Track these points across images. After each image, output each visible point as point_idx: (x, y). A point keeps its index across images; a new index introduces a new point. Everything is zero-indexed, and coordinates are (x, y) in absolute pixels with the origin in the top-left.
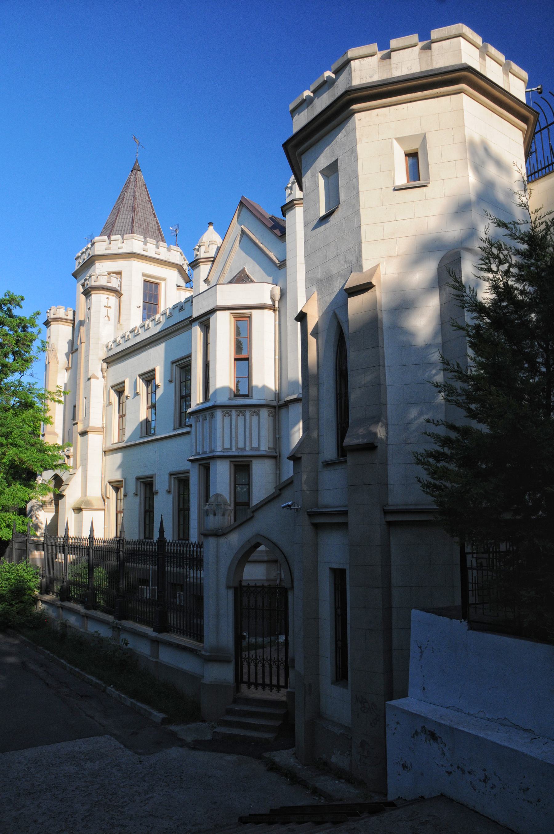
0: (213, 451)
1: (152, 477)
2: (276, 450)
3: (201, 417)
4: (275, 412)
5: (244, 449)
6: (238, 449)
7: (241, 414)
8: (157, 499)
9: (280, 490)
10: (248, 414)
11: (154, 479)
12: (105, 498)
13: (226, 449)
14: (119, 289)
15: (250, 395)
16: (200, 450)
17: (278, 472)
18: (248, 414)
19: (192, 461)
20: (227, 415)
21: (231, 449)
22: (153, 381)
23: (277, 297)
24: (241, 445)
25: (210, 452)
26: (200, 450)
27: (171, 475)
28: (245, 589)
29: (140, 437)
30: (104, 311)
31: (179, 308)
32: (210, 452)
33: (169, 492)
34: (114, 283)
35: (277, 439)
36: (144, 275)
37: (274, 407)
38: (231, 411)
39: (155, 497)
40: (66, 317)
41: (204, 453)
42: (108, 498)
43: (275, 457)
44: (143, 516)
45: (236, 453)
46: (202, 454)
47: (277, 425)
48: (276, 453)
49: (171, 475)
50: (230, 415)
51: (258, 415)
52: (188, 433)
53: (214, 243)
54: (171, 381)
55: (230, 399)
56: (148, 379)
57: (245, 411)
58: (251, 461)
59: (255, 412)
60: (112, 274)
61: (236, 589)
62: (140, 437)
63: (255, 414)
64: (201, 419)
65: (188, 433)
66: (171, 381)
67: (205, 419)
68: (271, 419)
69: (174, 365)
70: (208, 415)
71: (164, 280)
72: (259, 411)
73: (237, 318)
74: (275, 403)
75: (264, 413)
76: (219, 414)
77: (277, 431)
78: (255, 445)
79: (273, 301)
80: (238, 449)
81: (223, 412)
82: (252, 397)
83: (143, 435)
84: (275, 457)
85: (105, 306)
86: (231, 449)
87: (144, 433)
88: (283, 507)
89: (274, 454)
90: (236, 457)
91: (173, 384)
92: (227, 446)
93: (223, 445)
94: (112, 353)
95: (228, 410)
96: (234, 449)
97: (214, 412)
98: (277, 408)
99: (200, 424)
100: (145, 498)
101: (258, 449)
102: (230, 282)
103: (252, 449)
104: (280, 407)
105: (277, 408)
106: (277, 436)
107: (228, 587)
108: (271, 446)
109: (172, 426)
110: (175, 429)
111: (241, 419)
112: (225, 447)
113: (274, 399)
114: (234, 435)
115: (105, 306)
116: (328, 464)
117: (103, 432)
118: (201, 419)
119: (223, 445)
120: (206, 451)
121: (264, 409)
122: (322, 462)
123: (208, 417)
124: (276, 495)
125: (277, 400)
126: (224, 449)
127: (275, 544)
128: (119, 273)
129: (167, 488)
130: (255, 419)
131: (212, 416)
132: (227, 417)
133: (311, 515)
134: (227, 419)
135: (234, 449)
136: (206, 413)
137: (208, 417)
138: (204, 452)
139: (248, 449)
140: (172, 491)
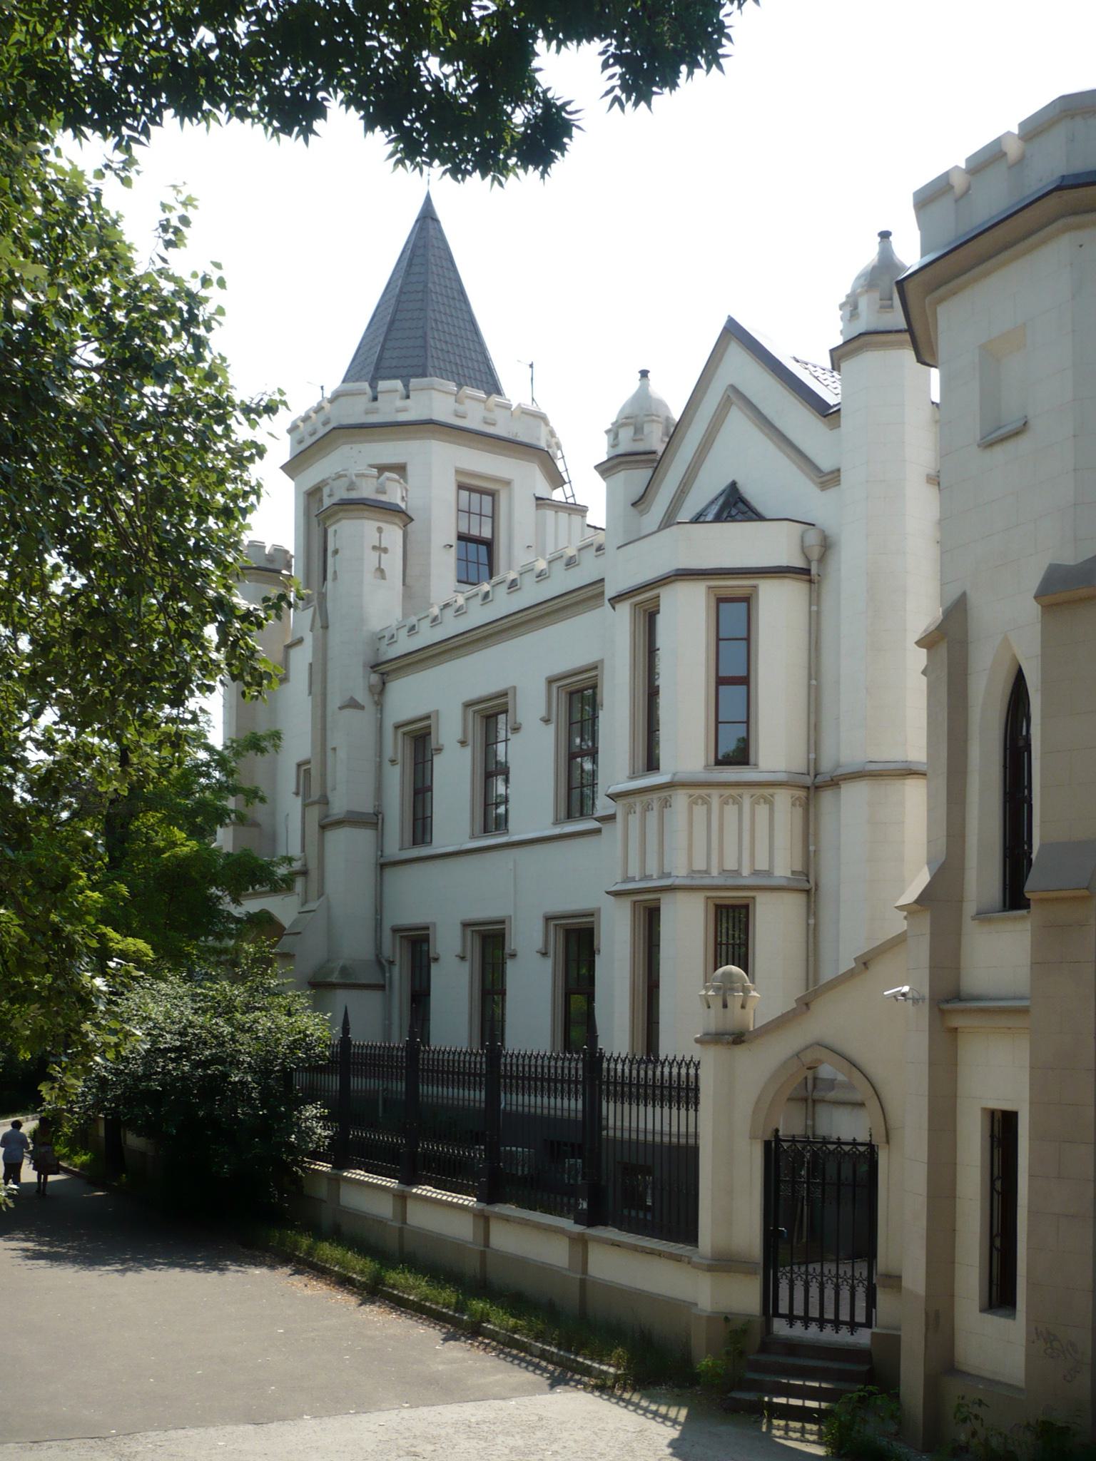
1: (503, 922)
5: (737, 873)
6: (723, 871)
11: (506, 926)
12: (382, 964)
22: (502, 718)
27: (548, 919)
30: (371, 558)
38: (709, 796)
39: (510, 965)
44: (477, 1002)
46: (640, 880)
49: (548, 919)
58: (754, 898)
76: (680, 799)
78: (762, 865)
80: (723, 871)
81: (690, 796)
85: (374, 548)
91: (552, 727)
97: (670, 796)
101: (769, 873)
103: (756, 873)
111: (731, 810)
115: (374, 548)
117: (377, 823)
120: (652, 876)
134: (700, 810)
138: (646, 876)
139: (746, 872)
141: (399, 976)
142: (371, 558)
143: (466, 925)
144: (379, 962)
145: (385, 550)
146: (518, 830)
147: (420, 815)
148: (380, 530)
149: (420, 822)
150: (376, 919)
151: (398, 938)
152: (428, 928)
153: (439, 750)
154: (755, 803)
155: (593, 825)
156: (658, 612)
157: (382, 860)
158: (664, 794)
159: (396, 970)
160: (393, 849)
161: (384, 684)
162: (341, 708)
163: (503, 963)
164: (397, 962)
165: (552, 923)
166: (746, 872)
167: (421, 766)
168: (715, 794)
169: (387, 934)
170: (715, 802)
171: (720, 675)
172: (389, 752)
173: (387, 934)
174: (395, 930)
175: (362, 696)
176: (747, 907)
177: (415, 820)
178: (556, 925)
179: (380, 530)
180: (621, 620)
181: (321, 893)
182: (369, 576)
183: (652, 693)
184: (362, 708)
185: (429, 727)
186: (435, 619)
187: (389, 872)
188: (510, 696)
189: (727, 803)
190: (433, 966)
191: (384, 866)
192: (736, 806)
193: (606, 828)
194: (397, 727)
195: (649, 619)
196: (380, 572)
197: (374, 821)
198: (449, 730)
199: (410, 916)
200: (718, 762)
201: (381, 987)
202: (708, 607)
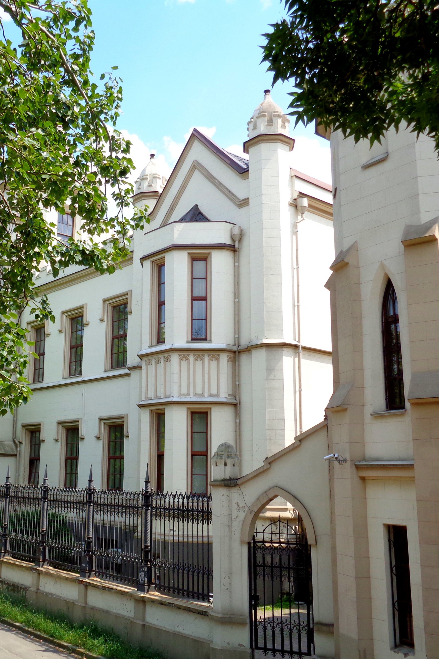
2: (235, 397)
3: (153, 360)
4: (235, 357)
5: (202, 395)
7: (199, 359)
8: (82, 446)
9: (300, 441)
10: (206, 359)
11: (80, 424)
12: (17, 443)
13: (184, 394)
15: (209, 338)
16: (151, 394)
17: (238, 421)
18: (206, 359)
19: (141, 406)
20: (184, 359)
21: (188, 395)
23: (237, 238)
24: (199, 391)
27: (101, 420)
28: (259, 545)
29: (63, 379)
32: (165, 398)
35: (237, 385)
37: (235, 352)
38: (188, 355)
39: (81, 444)
42: (20, 443)
43: (235, 405)
45: (194, 399)
47: (237, 370)
48: (236, 400)
49: (101, 420)
50: (187, 359)
51: (217, 360)
52: (128, 375)
53: (158, 176)
55: (188, 342)
56: (73, 317)
57: (203, 356)
58: (210, 408)
59: (213, 357)
61: (249, 544)
62: (63, 379)
63: (214, 359)
64: (153, 362)
65: (128, 375)
66: (102, 320)
67: (158, 362)
68: (230, 363)
69: (106, 304)
70: (162, 358)
72: (219, 355)
73: (194, 259)
74: (235, 348)
75: (224, 358)
76: (175, 358)
77: (237, 377)
78: (214, 391)
79: (234, 241)
81: (180, 356)
82: (211, 341)
83: (66, 376)
84: (235, 405)
86: (188, 395)
89: (234, 401)
90: (190, 403)
92: (184, 391)
93: (180, 390)
95: (186, 353)
96: (192, 395)
98: (237, 353)
99: (151, 368)
100: (67, 444)
101: (217, 395)
102: (182, 220)
103: (211, 395)
104: (239, 352)
105: (237, 353)
106: (237, 383)
107: (242, 542)
108: (230, 393)
109: (103, 368)
110: (106, 371)
111: (199, 363)
113: (233, 344)
114: (191, 380)
116: (377, 416)
118: (153, 362)
119: (180, 390)
121: (224, 354)
122: (371, 415)
123: (162, 361)
124: (295, 445)
125: (237, 345)
127: (295, 497)
129: (96, 432)
130: (214, 363)
131: (168, 359)
132: (184, 361)
133: (358, 467)
134: (184, 363)
135: (192, 395)
136: (160, 356)
137: (162, 361)
139: (206, 394)
140: (102, 437)
143: (59, 423)
146: (87, 374)
147: (37, 367)
149: (37, 371)
150: (14, 420)
151: (24, 430)
153: (49, 335)
155: (126, 371)
156: (164, 265)
158: (166, 355)
159: (23, 446)
163: (78, 444)
164: (23, 442)
166: (206, 394)
167: (39, 343)
169: (19, 427)
171: (193, 296)
174: (23, 426)
176: (206, 413)
177: (35, 370)
178: (105, 423)
183: (161, 304)
190: (42, 444)
192: (202, 361)
193: (135, 374)
199: (31, 420)
200: (193, 339)
201: (16, 455)
202: (188, 263)
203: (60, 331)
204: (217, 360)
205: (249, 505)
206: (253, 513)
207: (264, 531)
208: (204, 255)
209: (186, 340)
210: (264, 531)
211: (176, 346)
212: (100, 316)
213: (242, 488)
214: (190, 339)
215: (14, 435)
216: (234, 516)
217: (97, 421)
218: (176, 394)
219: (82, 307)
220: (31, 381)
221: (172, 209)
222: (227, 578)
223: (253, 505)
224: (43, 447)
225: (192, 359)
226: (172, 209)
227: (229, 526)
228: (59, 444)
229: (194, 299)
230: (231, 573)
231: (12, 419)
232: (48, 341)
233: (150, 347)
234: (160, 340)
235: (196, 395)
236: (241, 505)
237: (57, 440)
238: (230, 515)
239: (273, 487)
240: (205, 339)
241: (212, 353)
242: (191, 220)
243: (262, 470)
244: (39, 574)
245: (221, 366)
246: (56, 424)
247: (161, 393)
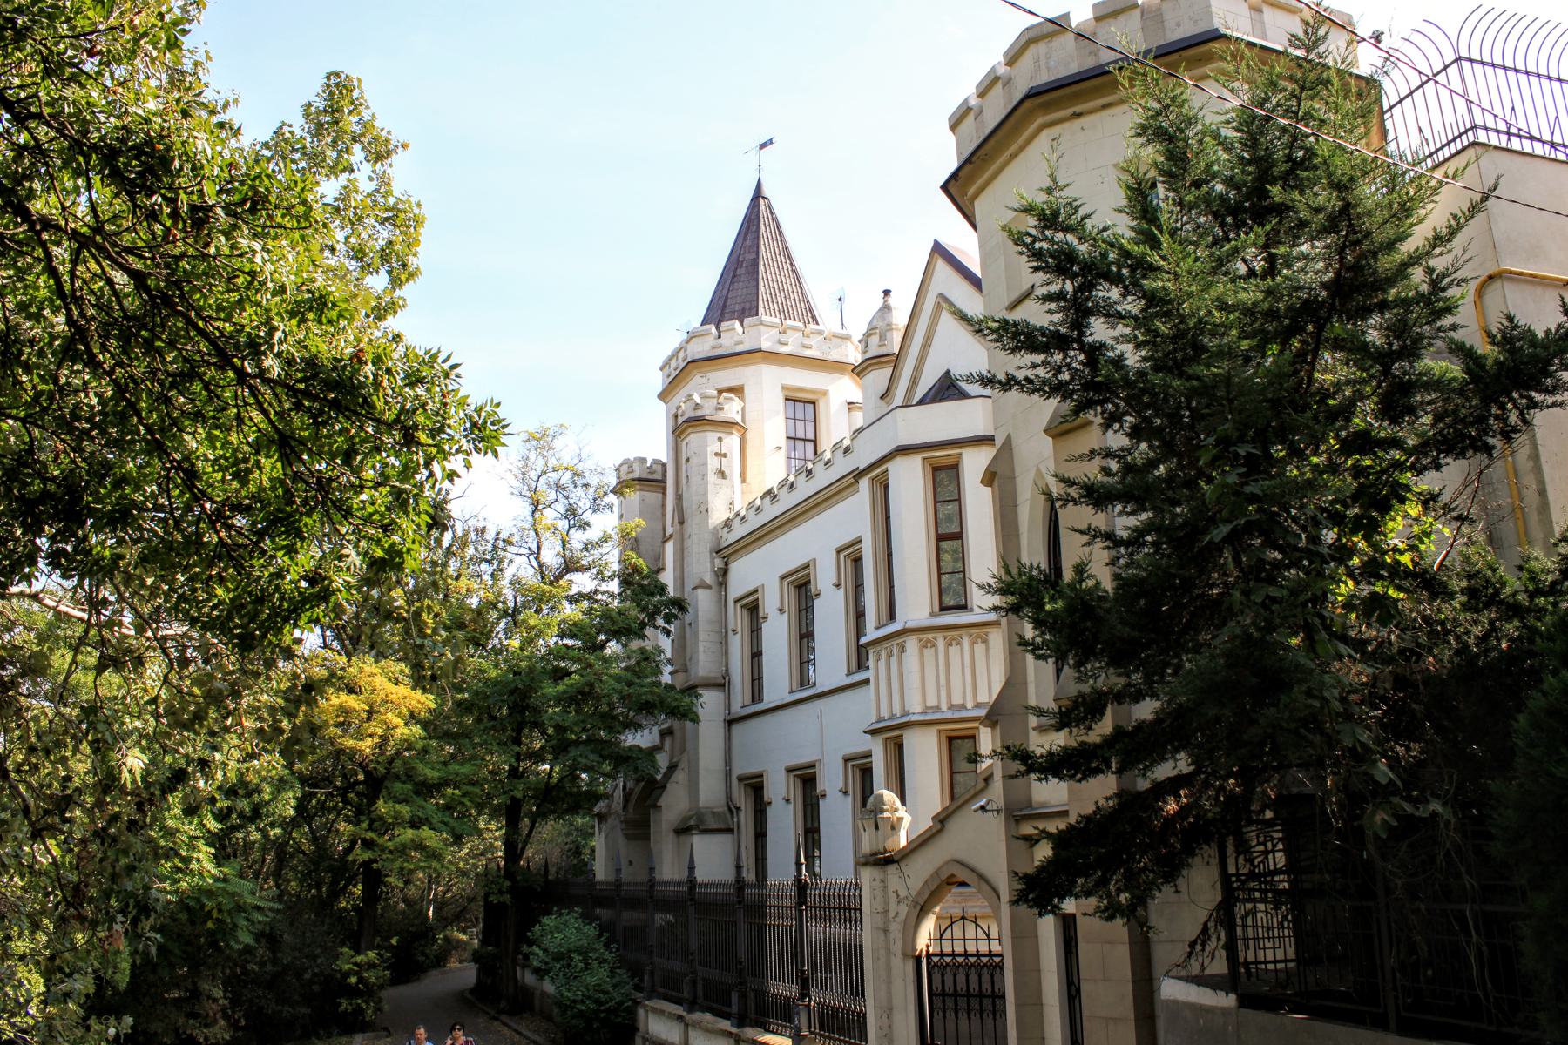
0: (906, 713)
5: (963, 707)
8: (824, 807)
10: (966, 642)
11: (817, 770)
12: (733, 810)
14: (739, 420)
16: (885, 713)
19: (873, 732)
21: (938, 707)
25: (902, 716)
26: (885, 713)
27: (846, 760)
28: (936, 959)
31: (842, 450)
32: (902, 716)
33: (845, 793)
34: (732, 410)
36: (784, 388)
38: (935, 638)
40: (651, 477)
41: (893, 717)
42: (738, 809)
45: (949, 715)
49: (846, 760)
51: (985, 641)
52: (867, 681)
54: (838, 586)
55: (932, 614)
59: (978, 636)
60: (725, 394)
64: (884, 654)
65: (867, 681)
69: (842, 555)
71: (825, 393)
72: (986, 634)
76: (912, 643)
83: (795, 688)
85: (716, 454)
86: (938, 707)
87: (796, 686)
88: (975, 811)
92: (932, 702)
94: (732, 537)
99: (882, 664)
112: (929, 704)
115: (716, 454)
118: (884, 654)
126: (927, 708)
128: (738, 391)
129: (841, 784)
130: (980, 648)
131: (903, 649)
135: (944, 707)
139: (969, 705)
141: (746, 819)
142: (713, 463)
143: (789, 770)
144: (730, 809)
145: (725, 455)
148: (720, 439)
152: (762, 776)
154: (973, 643)
157: (731, 717)
159: (742, 815)
160: (737, 709)
161: (726, 564)
162: (694, 589)
165: (850, 764)
168: (939, 635)
169: (735, 782)
170: (941, 643)
172: (731, 626)
173: (735, 782)
174: (741, 779)
175: (709, 578)
176: (973, 737)
177: (753, 681)
179: (720, 439)
180: (863, 494)
181: (683, 750)
182: (712, 478)
184: (709, 587)
185: (757, 600)
186: (759, 508)
187: (736, 728)
188: (811, 570)
189: (950, 645)
191: (730, 722)
194: (736, 601)
195: (882, 487)
196: (722, 474)
197: (721, 684)
198: (771, 602)
200: (944, 609)
201: (729, 830)
203: (781, 610)
204: (985, 641)
205: (914, 893)
206: (919, 908)
207: (941, 935)
208: (951, 461)
209: (928, 611)
210: (941, 935)
211: (910, 625)
212: (835, 580)
213: (903, 864)
214: (937, 609)
215: (729, 796)
216: (892, 914)
217: (841, 762)
218: (918, 709)
219: (807, 566)
220: (748, 700)
221: (914, 382)
222: (885, 1016)
223: (919, 894)
224: (770, 812)
225: (941, 643)
226: (914, 382)
227: (886, 931)
228: (791, 806)
229: (940, 538)
230: (891, 1009)
231: (723, 768)
232: (765, 627)
233: (877, 628)
234: (892, 617)
235: (952, 707)
236: (903, 893)
237: (788, 801)
238: (886, 911)
239: (947, 863)
240: (963, 607)
241: (975, 631)
242: (933, 401)
243: (930, 833)
244: (687, 1025)
245: (992, 652)
246: (784, 772)
247: (897, 710)
